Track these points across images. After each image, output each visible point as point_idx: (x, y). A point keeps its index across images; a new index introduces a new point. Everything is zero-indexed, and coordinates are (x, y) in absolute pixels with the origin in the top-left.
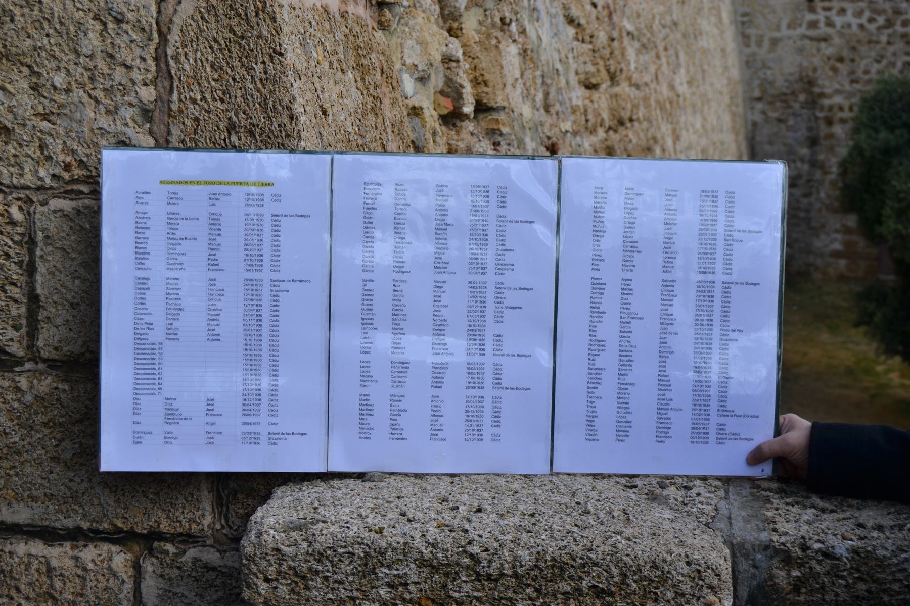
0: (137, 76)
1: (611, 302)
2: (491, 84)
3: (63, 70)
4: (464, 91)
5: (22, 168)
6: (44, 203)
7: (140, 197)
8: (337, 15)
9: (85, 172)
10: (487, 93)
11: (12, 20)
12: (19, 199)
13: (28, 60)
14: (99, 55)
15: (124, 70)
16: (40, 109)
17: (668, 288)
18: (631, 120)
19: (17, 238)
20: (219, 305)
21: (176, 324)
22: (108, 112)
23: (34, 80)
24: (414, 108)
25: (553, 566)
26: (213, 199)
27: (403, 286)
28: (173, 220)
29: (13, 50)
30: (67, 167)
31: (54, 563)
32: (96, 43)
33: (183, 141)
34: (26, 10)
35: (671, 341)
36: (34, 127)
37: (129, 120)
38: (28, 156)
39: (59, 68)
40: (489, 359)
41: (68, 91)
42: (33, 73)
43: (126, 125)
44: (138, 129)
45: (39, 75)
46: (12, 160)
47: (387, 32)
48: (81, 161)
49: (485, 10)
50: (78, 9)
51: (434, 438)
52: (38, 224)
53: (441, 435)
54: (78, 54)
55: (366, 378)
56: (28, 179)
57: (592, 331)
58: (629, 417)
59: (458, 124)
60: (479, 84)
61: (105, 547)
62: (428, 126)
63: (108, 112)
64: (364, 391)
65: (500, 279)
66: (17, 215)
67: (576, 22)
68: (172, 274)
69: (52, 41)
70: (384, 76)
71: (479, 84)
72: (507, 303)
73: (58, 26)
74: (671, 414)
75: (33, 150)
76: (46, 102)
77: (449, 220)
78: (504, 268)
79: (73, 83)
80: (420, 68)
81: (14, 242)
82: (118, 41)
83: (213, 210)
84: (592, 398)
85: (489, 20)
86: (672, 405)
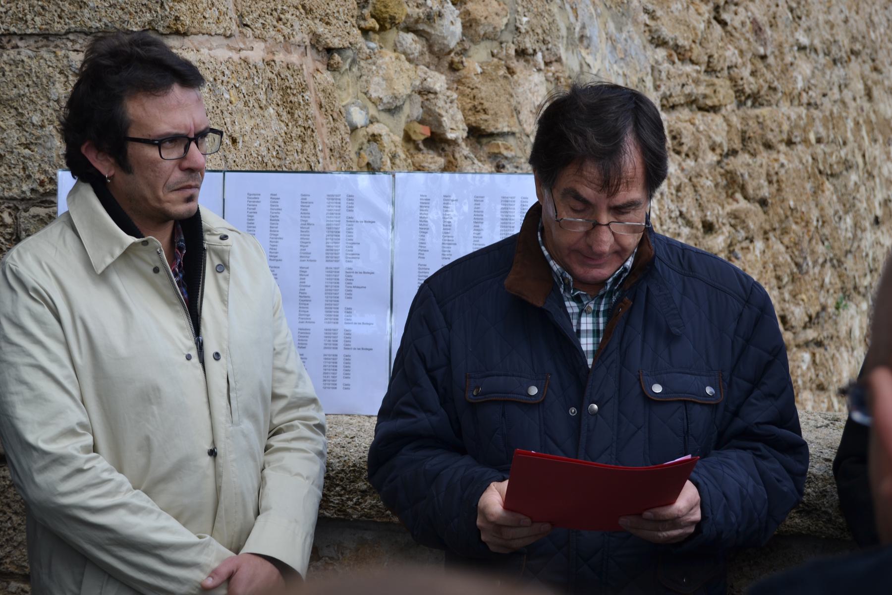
2: (491, 112)
5: (11, 185)
6: (26, 210)
8: (260, 65)
10: (486, 121)
13: (15, 104)
16: (23, 140)
18: (790, 143)
19: (7, 237)
23: (19, 119)
24: (373, 135)
25: (354, 471)
30: (42, 183)
34: (13, 67)
38: (15, 175)
39: (36, 110)
40: (341, 327)
41: (42, 127)
45: (22, 115)
47: (337, 73)
49: (501, 43)
50: (49, 66)
52: (23, 226)
54: (49, 100)
56: (15, 192)
59: (447, 148)
62: (387, 150)
66: (8, 220)
67: (671, 43)
69: (31, 90)
70: (323, 109)
71: (478, 112)
72: (354, 283)
73: (35, 79)
75: (18, 171)
76: (27, 135)
77: (310, 221)
80: (385, 100)
81: (6, 240)
85: (504, 52)
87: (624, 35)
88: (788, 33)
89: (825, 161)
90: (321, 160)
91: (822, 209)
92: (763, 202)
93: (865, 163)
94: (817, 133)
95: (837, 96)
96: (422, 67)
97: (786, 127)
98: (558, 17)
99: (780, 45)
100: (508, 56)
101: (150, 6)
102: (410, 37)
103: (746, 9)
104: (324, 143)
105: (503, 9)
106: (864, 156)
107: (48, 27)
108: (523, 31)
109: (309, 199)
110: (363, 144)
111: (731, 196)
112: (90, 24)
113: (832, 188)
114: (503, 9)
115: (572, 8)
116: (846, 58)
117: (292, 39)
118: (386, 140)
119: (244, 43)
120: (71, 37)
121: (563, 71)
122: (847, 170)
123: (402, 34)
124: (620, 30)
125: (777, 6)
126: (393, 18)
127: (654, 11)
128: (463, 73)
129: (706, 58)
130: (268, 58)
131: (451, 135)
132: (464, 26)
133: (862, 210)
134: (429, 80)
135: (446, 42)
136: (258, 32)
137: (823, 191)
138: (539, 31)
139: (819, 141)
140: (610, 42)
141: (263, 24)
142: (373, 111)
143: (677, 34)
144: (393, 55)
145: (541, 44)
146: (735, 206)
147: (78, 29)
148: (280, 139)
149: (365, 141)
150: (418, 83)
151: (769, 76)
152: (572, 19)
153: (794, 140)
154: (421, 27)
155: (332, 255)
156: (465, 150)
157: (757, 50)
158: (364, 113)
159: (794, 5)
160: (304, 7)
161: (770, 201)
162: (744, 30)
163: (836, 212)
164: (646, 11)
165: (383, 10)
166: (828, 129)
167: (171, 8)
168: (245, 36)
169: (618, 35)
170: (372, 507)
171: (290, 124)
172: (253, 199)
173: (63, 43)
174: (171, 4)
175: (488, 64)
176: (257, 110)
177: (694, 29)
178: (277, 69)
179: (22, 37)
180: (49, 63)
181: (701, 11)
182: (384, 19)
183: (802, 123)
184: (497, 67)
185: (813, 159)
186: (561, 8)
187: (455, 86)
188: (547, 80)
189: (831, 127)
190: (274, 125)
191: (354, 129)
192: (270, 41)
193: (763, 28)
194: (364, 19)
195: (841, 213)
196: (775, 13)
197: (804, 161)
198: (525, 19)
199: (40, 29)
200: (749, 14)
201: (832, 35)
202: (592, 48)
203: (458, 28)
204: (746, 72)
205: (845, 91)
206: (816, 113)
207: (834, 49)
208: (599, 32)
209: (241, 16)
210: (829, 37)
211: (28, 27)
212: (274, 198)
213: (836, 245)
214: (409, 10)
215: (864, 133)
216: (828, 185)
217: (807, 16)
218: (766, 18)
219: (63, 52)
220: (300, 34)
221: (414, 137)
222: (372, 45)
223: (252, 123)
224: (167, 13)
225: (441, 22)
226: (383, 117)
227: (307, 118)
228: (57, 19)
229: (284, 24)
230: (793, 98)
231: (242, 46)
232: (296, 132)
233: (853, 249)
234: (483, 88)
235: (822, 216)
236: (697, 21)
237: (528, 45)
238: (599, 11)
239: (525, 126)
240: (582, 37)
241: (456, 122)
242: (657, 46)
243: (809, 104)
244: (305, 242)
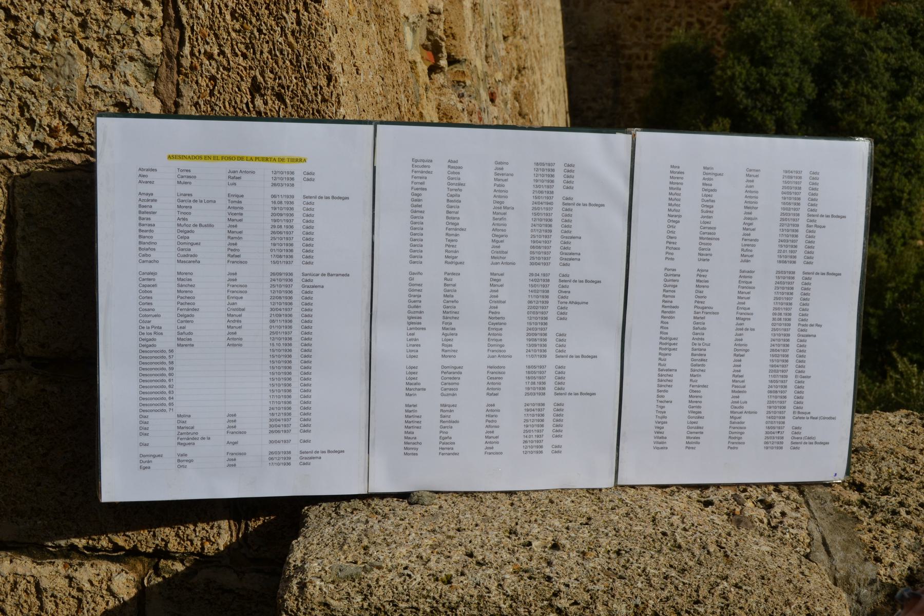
0: (140, 23)
1: (685, 296)
2: (458, 37)
3: (47, 14)
7: (144, 174)
9: (75, 139)
15: (123, 16)
16: (20, 61)
17: (746, 278)
20: (240, 304)
21: (189, 327)
22: (102, 66)
23: (11, 25)
26: (234, 177)
27: (455, 279)
28: (184, 203)
30: (53, 132)
31: (45, 583)
33: (196, 104)
35: (747, 337)
36: (11, 83)
37: (129, 77)
40: (551, 362)
41: (53, 40)
43: (126, 83)
45: (16, 19)
48: (70, 126)
51: (489, 451)
53: (497, 448)
55: (412, 386)
57: (664, 327)
58: (701, 423)
61: (104, 565)
63: (102, 66)
64: (411, 400)
65: (565, 270)
68: (184, 268)
72: (571, 297)
74: (745, 418)
76: (27, 53)
77: (508, 202)
78: (568, 257)
79: (60, 31)
83: (233, 190)
84: (662, 402)
86: (747, 408)
109: (507, 169)
155: (539, 253)
172: (421, 167)
212: (454, 167)
244: (498, 236)
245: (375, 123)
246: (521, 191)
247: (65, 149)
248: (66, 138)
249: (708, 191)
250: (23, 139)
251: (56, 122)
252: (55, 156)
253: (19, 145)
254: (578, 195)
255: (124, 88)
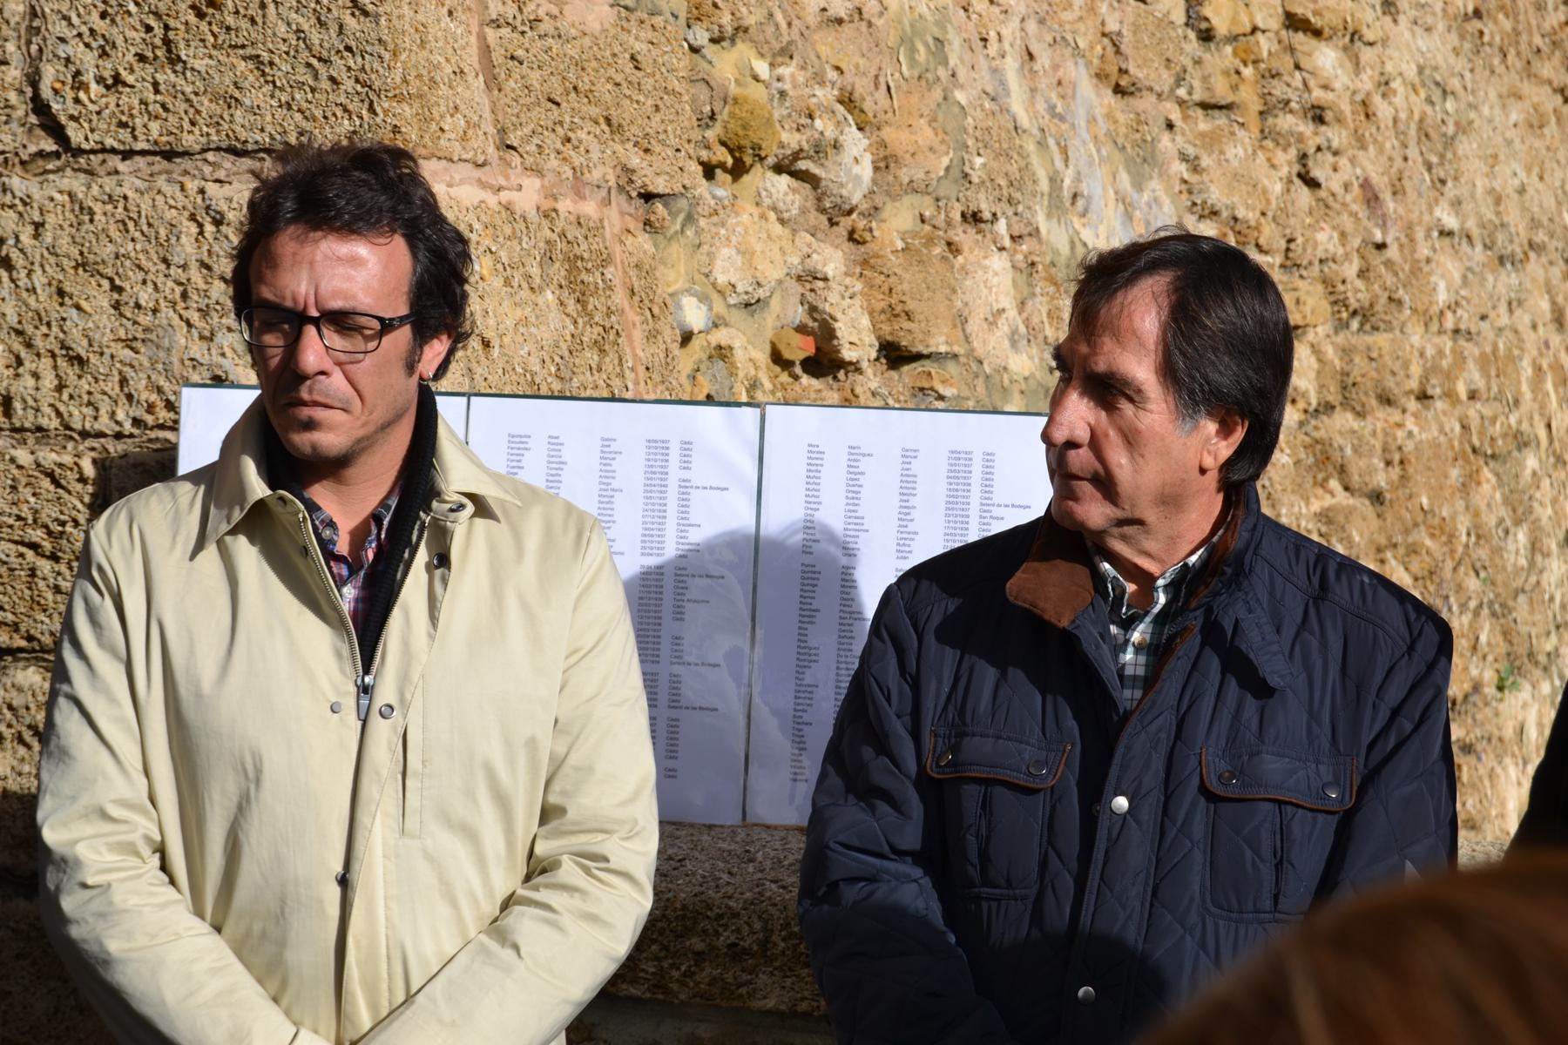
2: (917, 317)
3: (149, 284)
4: (836, 325)
5: (97, 409)
8: (532, 215)
9: (172, 415)
11: (91, 221)
12: (93, 449)
13: (109, 271)
14: (194, 266)
16: (122, 333)
18: (1423, 397)
22: (202, 337)
23: (116, 296)
24: (720, 347)
25: (684, 917)
29: (91, 258)
30: (150, 408)
32: (189, 250)
36: (112, 357)
38: (105, 393)
41: (155, 311)
42: (116, 289)
43: (223, 355)
44: (237, 361)
45: (120, 290)
46: (86, 397)
47: (660, 237)
48: (168, 401)
52: (115, 482)
54: (168, 266)
56: (104, 424)
60: (896, 316)
62: (741, 374)
63: (202, 337)
67: (1225, 214)
69: (138, 247)
70: (637, 299)
71: (896, 316)
73: (145, 228)
75: (112, 386)
76: (129, 324)
79: (161, 301)
80: (740, 289)
82: (216, 248)
87: (1146, 197)
88: (1424, 208)
89: (1481, 433)
90: (630, 386)
91: (1477, 514)
92: (1377, 497)
93: (1551, 440)
94: (1468, 382)
95: (1504, 320)
96: (804, 234)
97: (1416, 370)
98: (1035, 161)
99: (1410, 227)
100: (949, 223)
101: (350, 107)
102: (785, 180)
103: (1353, 161)
104: (635, 355)
105: (943, 141)
106: (1549, 426)
107: (171, 139)
108: (976, 180)
109: (614, 447)
110: (700, 361)
111: (1323, 484)
112: (243, 135)
113: (1493, 480)
114: (943, 141)
115: (1058, 144)
116: (1520, 255)
117: (587, 175)
118: (739, 355)
119: (507, 178)
120: (210, 156)
121: (1043, 254)
122: (1519, 450)
123: (770, 174)
124: (1139, 187)
125: (1406, 159)
126: (756, 147)
127: (1197, 158)
128: (872, 247)
129: (1283, 244)
130: (547, 204)
131: (848, 354)
132: (876, 169)
133: (1545, 521)
134: (815, 256)
135: (844, 192)
136: (530, 160)
137: (1479, 483)
138: (1003, 182)
139: (1473, 396)
140: (1121, 206)
141: (539, 146)
142: (719, 306)
143: (1235, 199)
144: (756, 211)
145: (1004, 205)
146: (1328, 501)
147: (224, 145)
148: (564, 346)
149: (704, 357)
150: (796, 260)
151: (1390, 280)
152: (1059, 164)
153: (1430, 392)
154: (802, 165)
156: (872, 379)
157: (1370, 232)
158: (704, 308)
159: (1434, 159)
160: (608, 121)
161: (1388, 496)
162: (1349, 198)
163: (1501, 521)
164: (1184, 158)
165: (741, 133)
166: (1488, 377)
167: (386, 112)
168: (509, 165)
169: (1135, 196)
170: (713, 981)
171: (580, 321)
173: (197, 168)
174: (386, 105)
175: (915, 235)
176: (525, 294)
177: (1265, 191)
178: (560, 225)
179: (127, 155)
180: (171, 202)
181: (1276, 162)
182: (740, 148)
183: (1445, 363)
184: (930, 241)
185: (1463, 427)
186: (1042, 144)
187: (858, 270)
188: (1013, 267)
189: (1493, 373)
190: (551, 319)
191: (687, 338)
192: (550, 177)
193: (1381, 196)
194: (708, 147)
195: (1508, 522)
196: (1400, 172)
197: (1447, 429)
198: (979, 161)
199: (156, 143)
200: (1358, 171)
201: (1498, 214)
202: (1092, 216)
203: (866, 171)
204: (1351, 270)
205: (1518, 313)
206: (1471, 350)
207: (1500, 238)
208: (1104, 189)
209: (502, 131)
210: (1490, 215)
211: (135, 138)
212: (555, 443)
213: (1500, 578)
214: (785, 137)
215: (1549, 386)
216: (1486, 473)
217: (1456, 179)
218: (1386, 179)
219: (196, 182)
220: (601, 168)
221: (787, 355)
222: (720, 192)
223: (519, 313)
224: (378, 120)
225: (838, 159)
226: (737, 316)
227: (609, 313)
228: (186, 125)
229: (575, 148)
230: (1430, 319)
231: (504, 183)
232: (591, 334)
233: (1527, 588)
234: (907, 276)
235: (1477, 527)
236: (1269, 177)
237: (984, 206)
238: (1104, 153)
239: (975, 344)
240: (1075, 196)
241: (859, 332)
242: (1201, 217)
243: (1457, 331)
245: (469, 395)
246: (631, 470)
247: (162, 427)
248: (163, 415)
249: (854, 475)
250: (121, 416)
251: (154, 397)
252: (153, 434)
253: (117, 423)
254: (698, 475)
255: (220, 359)
